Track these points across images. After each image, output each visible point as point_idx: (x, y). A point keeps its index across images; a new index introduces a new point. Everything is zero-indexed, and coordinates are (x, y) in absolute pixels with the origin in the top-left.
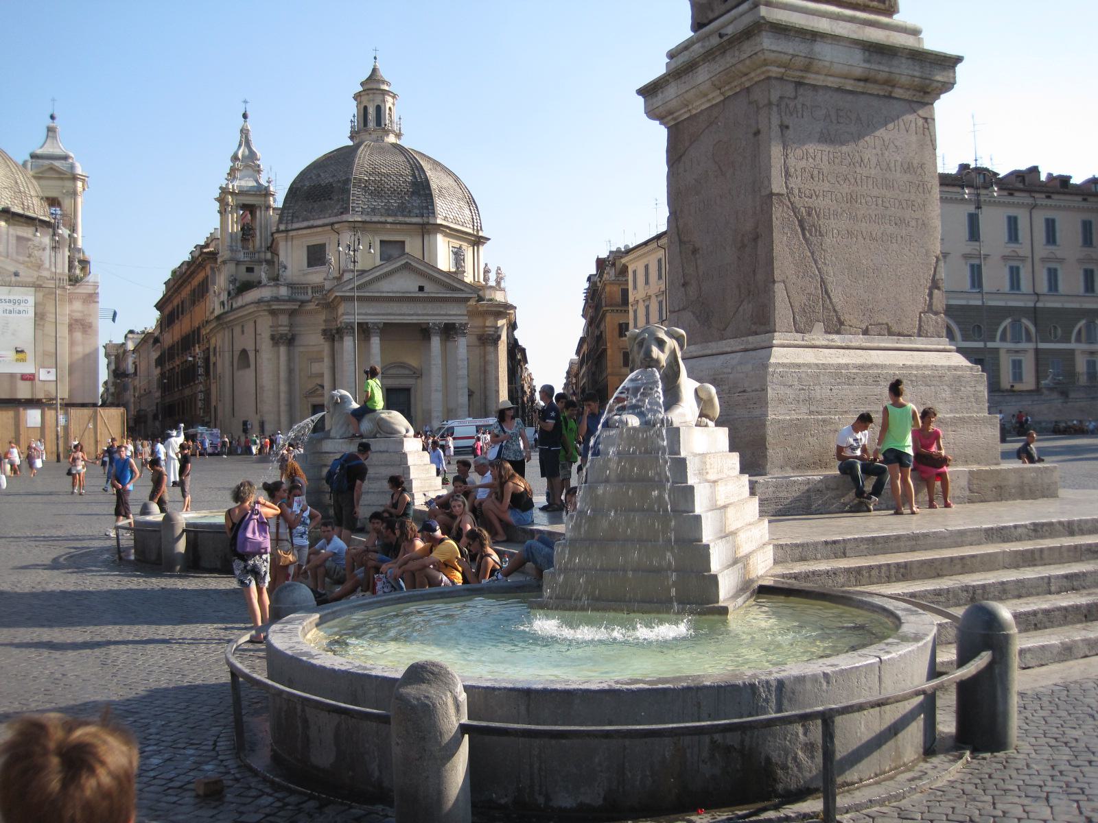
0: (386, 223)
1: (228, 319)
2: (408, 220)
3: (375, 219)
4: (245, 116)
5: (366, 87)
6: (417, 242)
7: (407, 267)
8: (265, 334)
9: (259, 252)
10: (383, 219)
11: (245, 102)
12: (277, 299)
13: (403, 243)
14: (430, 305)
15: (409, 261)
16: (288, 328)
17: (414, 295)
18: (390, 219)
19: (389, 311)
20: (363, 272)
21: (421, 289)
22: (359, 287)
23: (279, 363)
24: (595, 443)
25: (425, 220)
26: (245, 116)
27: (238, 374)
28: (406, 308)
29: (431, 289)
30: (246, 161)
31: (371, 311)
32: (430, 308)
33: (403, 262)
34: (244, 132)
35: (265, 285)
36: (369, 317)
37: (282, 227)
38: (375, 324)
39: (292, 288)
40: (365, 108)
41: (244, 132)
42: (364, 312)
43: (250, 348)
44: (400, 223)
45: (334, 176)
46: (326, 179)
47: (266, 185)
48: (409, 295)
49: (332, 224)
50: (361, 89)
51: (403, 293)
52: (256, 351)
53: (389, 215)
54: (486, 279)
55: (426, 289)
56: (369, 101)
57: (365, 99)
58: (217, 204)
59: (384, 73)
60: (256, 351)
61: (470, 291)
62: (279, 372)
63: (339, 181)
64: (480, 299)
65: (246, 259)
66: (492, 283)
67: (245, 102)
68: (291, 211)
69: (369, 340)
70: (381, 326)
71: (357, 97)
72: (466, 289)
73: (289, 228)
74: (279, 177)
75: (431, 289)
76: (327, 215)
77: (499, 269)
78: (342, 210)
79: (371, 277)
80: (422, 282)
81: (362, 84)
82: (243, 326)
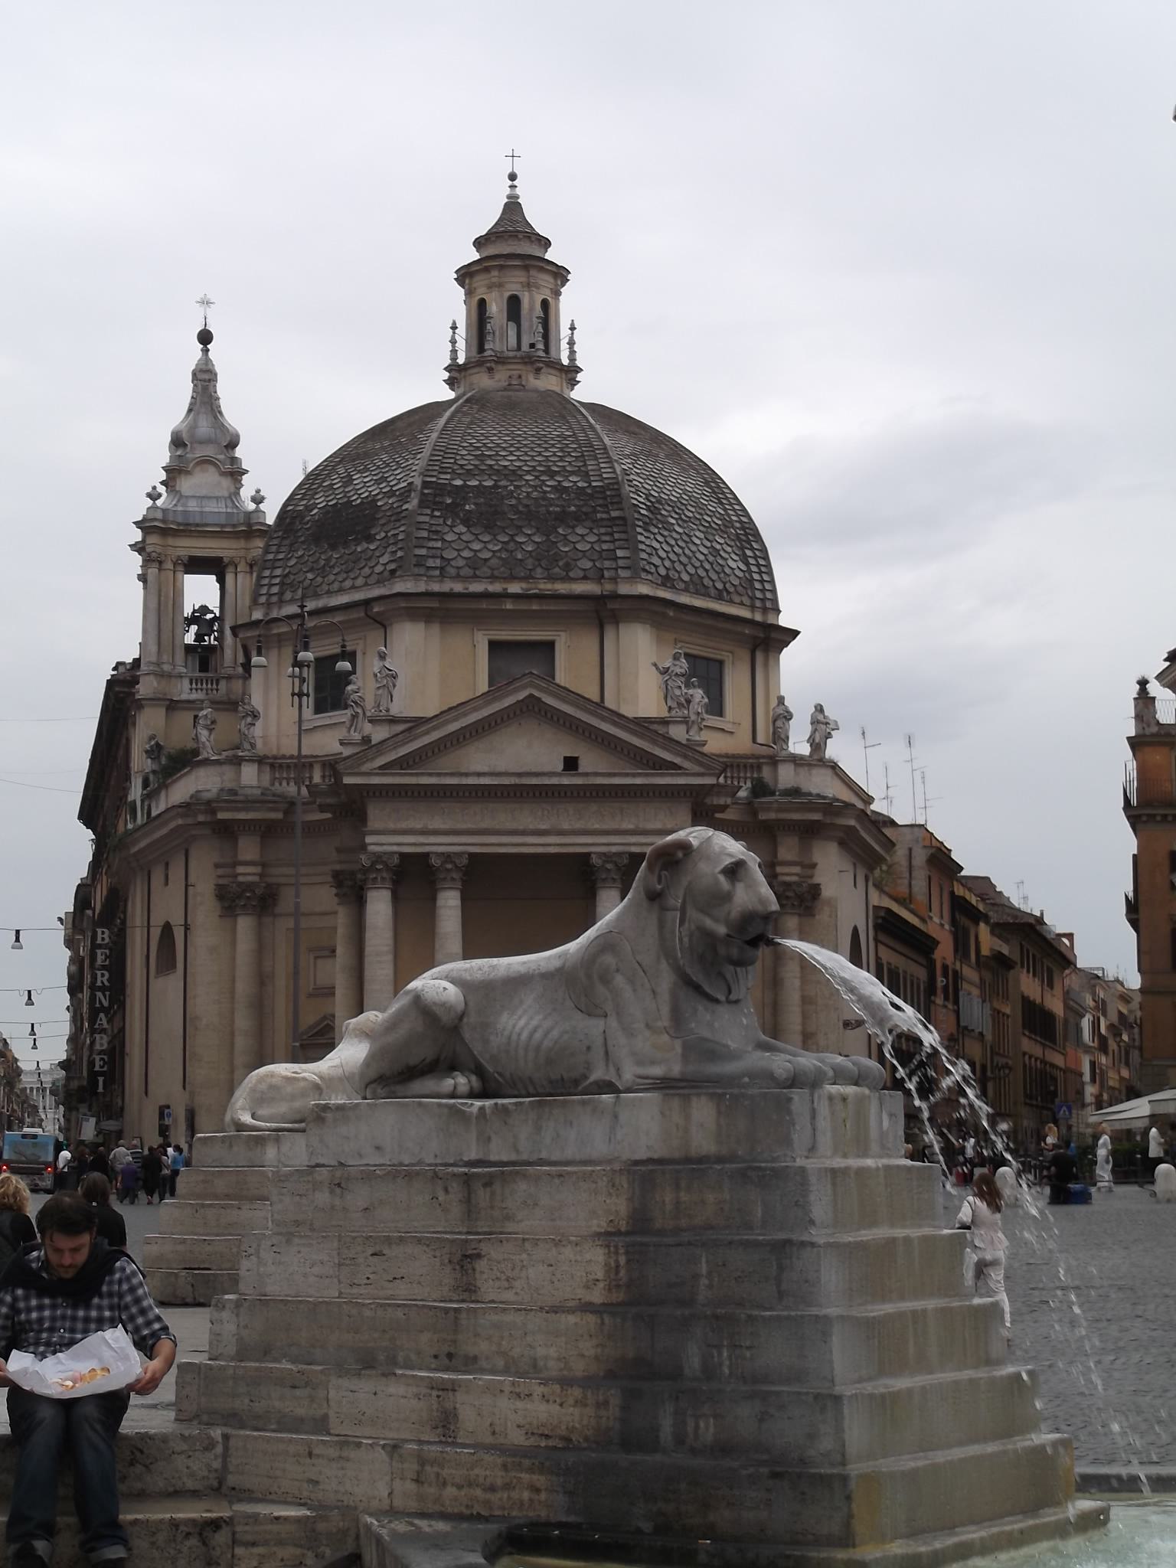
0: (505, 595)
1: (136, 849)
2: (562, 588)
3: (476, 587)
4: (205, 338)
5: (491, 251)
6: (587, 643)
7: (532, 709)
8: (204, 886)
9: (229, 678)
10: (496, 588)
11: (206, 302)
12: (232, 797)
13: (550, 646)
14: (594, 807)
15: (537, 694)
16: (258, 870)
17: (555, 781)
18: (515, 588)
19: (485, 824)
20: (417, 723)
21: (571, 764)
22: (402, 764)
23: (234, 959)
24: (340, 1108)
25: (609, 587)
26: (205, 338)
27: (157, 984)
28: (527, 817)
29: (595, 765)
30: (204, 444)
31: (437, 823)
32: (595, 817)
33: (521, 695)
34: (204, 378)
35: (207, 762)
36: (432, 839)
37: (257, 615)
38: (447, 857)
39: (272, 766)
40: (482, 303)
41: (204, 378)
42: (419, 826)
43: (177, 920)
44: (540, 597)
45: (384, 479)
46: (364, 486)
47: (252, 506)
48: (534, 781)
49: (367, 603)
50: (476, 256)
51: (520, 775)
52: (187, 927)
53: (512, 578)
54: (780, 737)
55: (584, 766)
56: (490, 287)
57: (480, 281)
58: (138, 559)
59: (537, 218)
60: (187, 927)
61: (697, 769)
62: (233, 981)
63: (391, 493)
64: (761, 789)
65: (194, 696)
66: (799, 744)
67: (206, 302)
68: (278, 572)
69: (434, 899)
70: (396, 860)
71: (465, 275)
72: (686, 764)
73: (274, 614)
74: (271, 480)
75: (595, 765)
76: (360, 582)
77: (819, 709)
78: (392, 566)
79: (435, 735)
80: (569, 747)
81: (479, 243)
82: (167, 864)
